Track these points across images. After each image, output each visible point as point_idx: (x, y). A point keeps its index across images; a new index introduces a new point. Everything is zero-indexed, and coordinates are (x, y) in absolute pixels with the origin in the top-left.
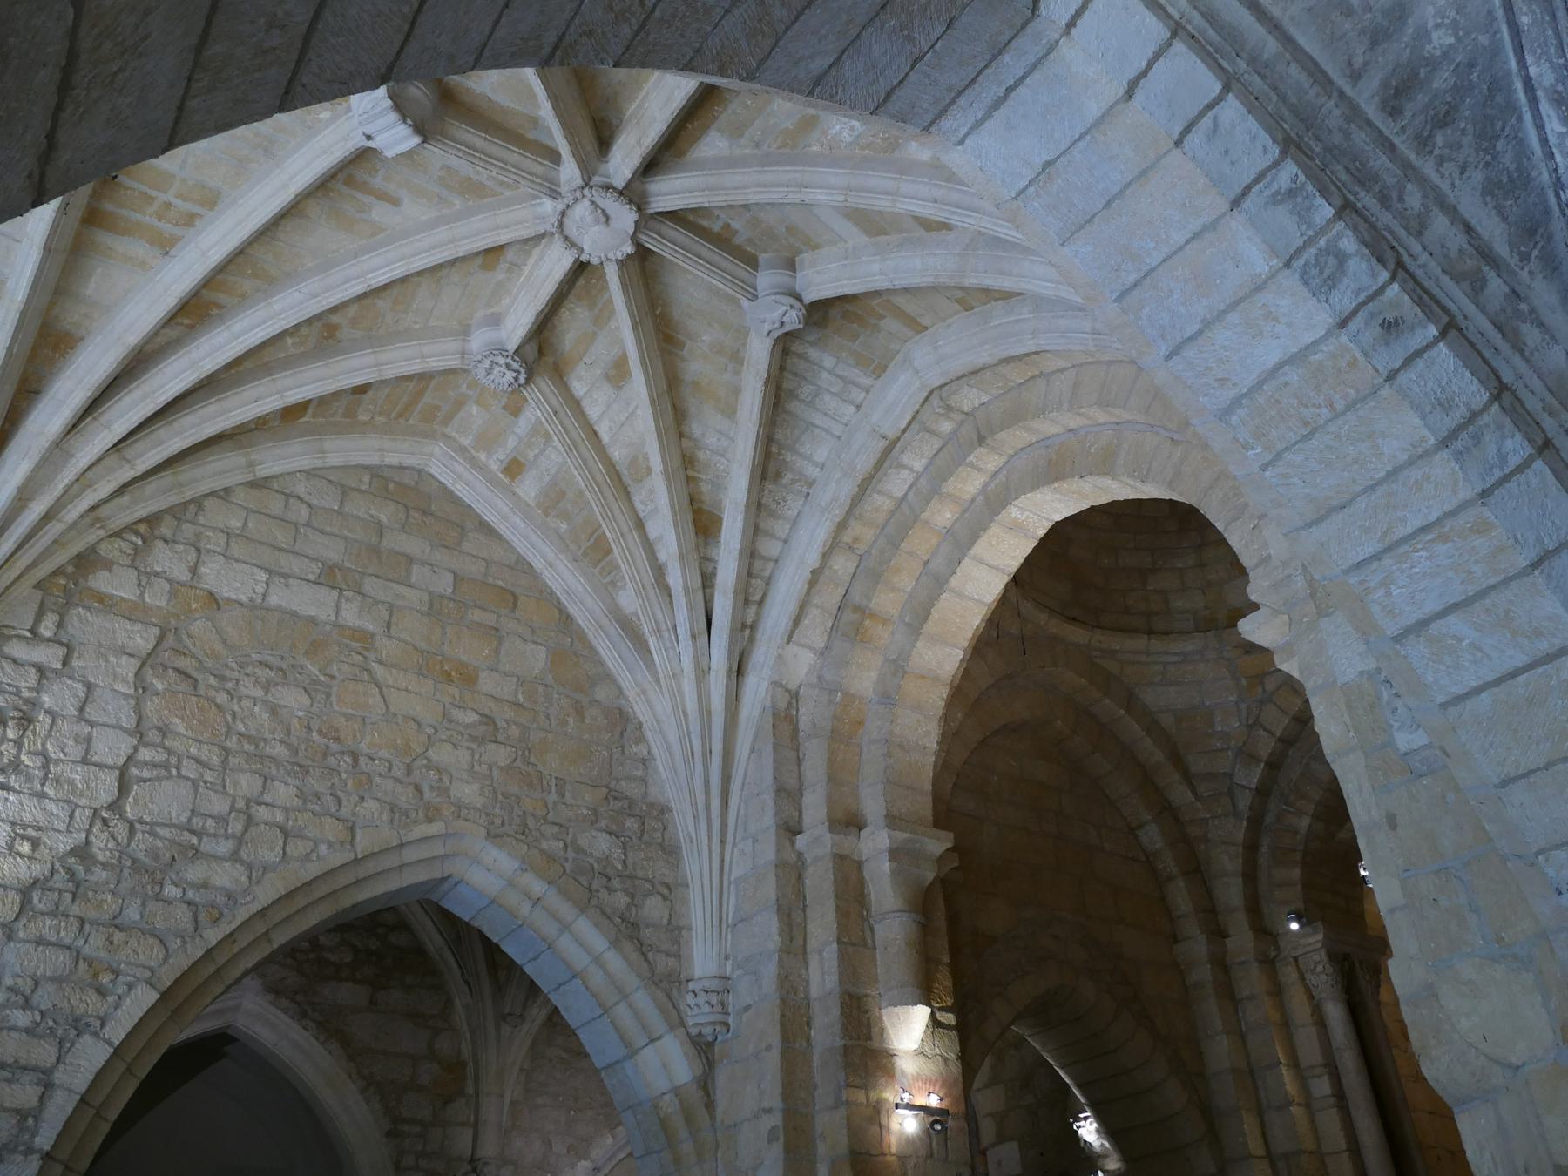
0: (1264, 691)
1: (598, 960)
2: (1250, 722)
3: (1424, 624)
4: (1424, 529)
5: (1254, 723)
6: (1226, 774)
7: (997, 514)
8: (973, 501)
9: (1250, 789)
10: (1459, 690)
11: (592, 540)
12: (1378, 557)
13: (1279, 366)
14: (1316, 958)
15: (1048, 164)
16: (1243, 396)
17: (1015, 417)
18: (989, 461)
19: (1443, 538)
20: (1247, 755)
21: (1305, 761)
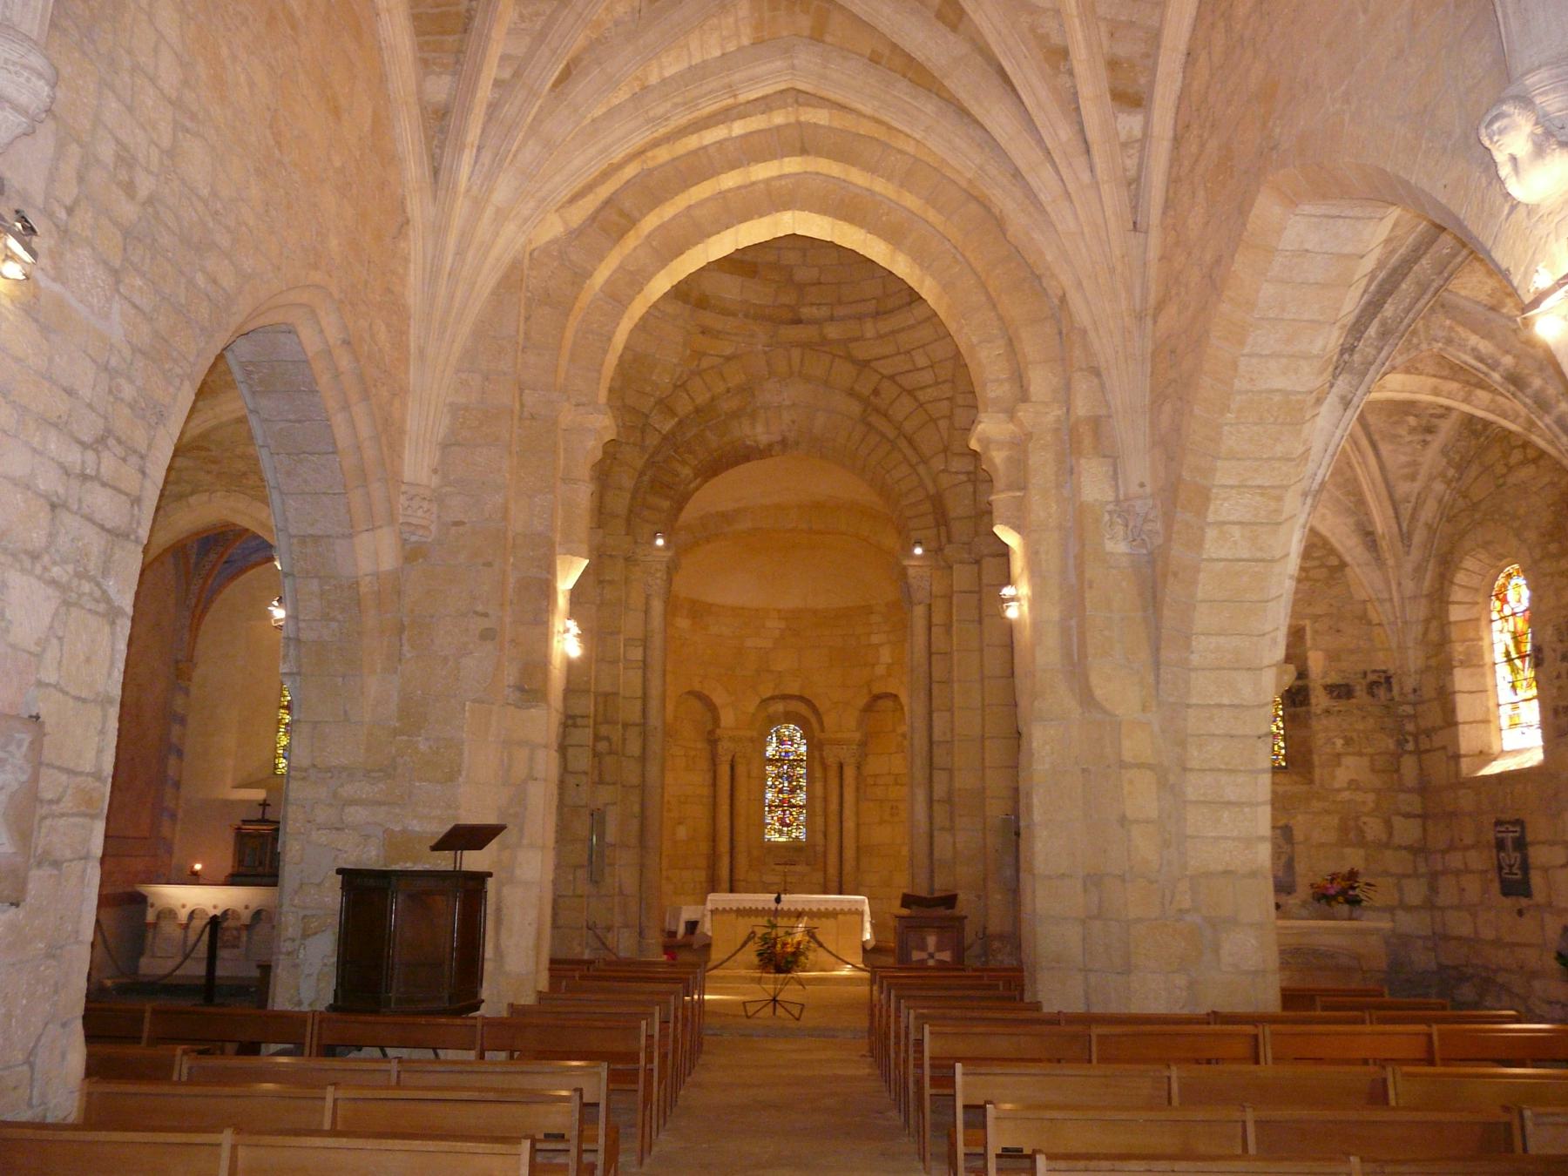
0: (698, 366)
1: (359, 448)
2: (679, 383)
3: (1224, 523)
4: (1259, 487)
5: (680, 386)
6: (643, 414)
7: (777, 211)
8: (753, 184)
9: (660, 432)
10: (1214, 556)
11: (436, 11)
12: (1232, 487)
13: (1278, 390)
14: (659, 567)
15: (1307, 251)
16: (1252, 391)
17: (842, 154)
18: (792, 165)
19: (1262, 495)
20: (665, 405)
21: (702, 427)
